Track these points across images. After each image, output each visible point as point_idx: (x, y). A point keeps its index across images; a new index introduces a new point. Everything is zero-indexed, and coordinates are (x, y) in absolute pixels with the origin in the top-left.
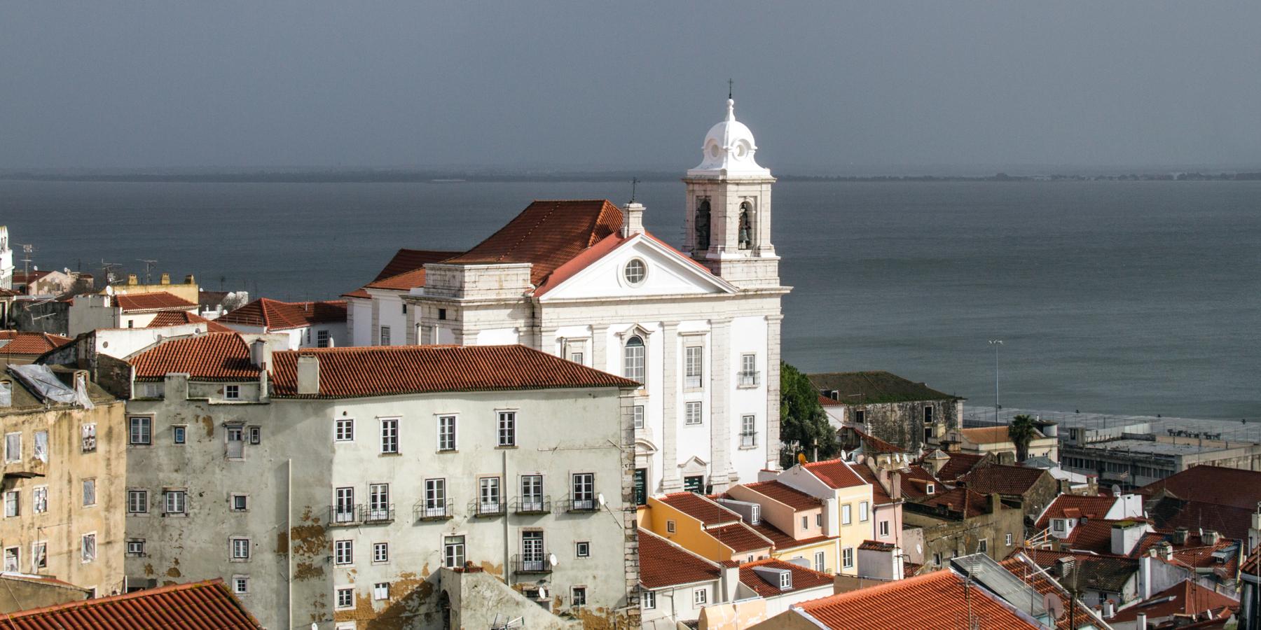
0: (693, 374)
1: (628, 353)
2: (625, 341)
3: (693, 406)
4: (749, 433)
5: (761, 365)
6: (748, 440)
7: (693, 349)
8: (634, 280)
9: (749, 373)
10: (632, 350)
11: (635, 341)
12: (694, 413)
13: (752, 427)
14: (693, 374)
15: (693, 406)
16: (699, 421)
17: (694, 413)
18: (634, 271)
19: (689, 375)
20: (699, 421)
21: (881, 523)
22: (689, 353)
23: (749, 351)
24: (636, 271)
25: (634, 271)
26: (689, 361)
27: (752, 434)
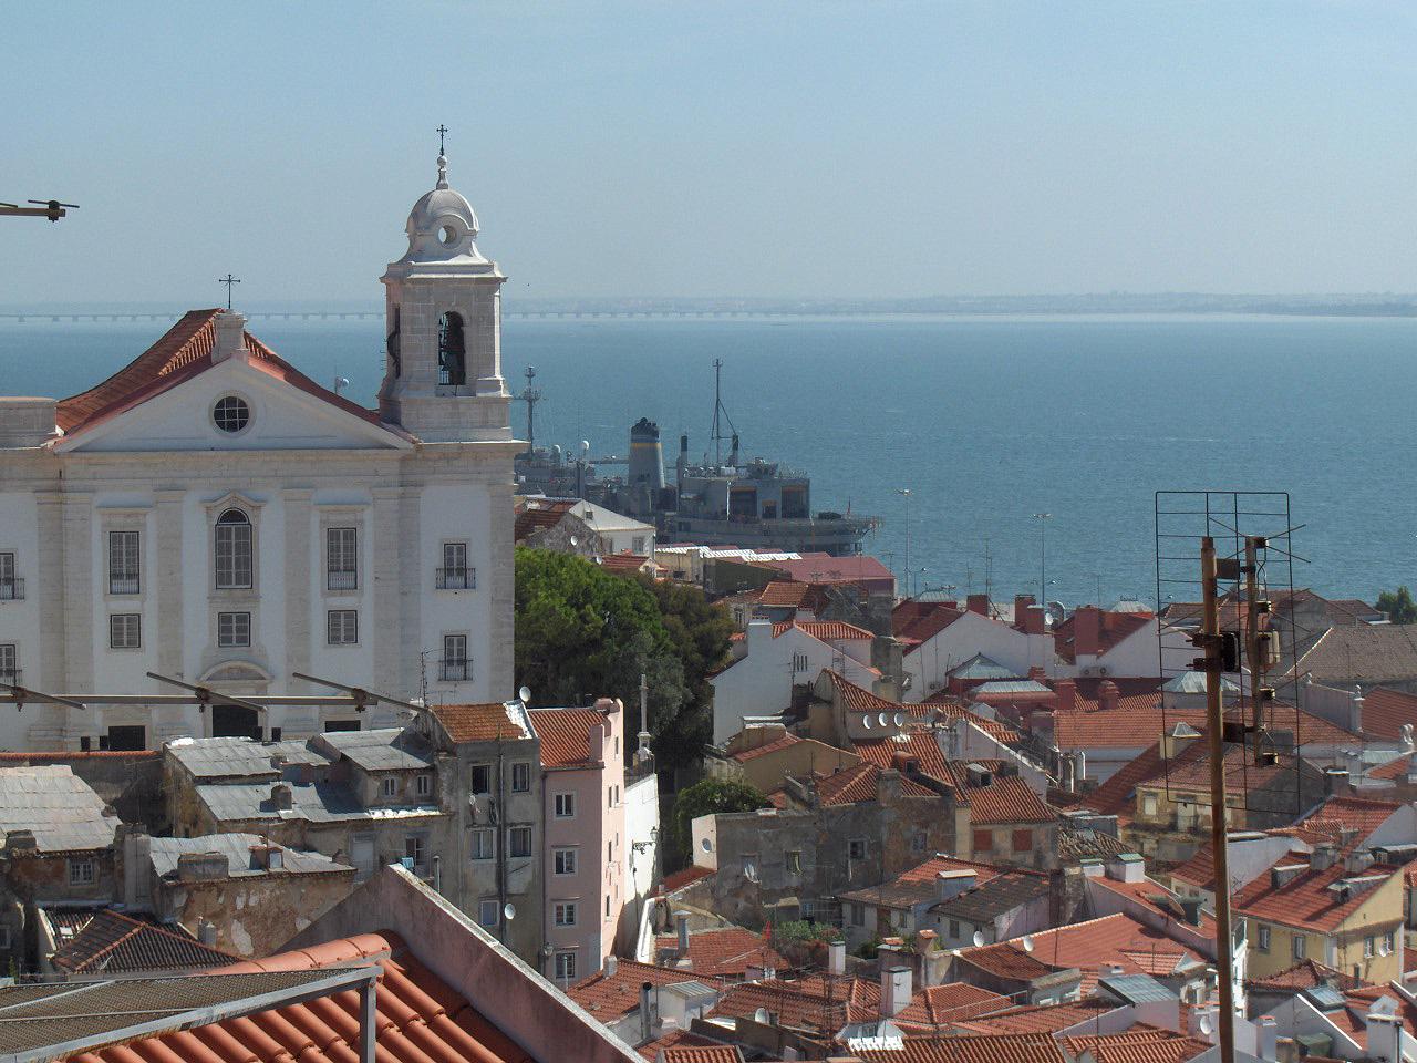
0: (342, 567)
1: (221, 534)
2: (216, 515)
3: (342, 616)
4: (456, 656)
5: (479, 558)
6: (456, 671)
7: (341, 532)
8: (233, 427)
9: (456, 568)
10: (229, 530)
11: (233, 516)
12: (342, 628)
13: (463, 651)
14: (342, 567)
15: (342, 616)
16: (352, 638)
17: (342, 628)
18: (232, 414)
19: (331, 570)
20: (352, 638)
21: (559, 799)
22: (332, 535)
23: (455, 536)
24: (231, 415)
25: (232, 414)
26: (332, 549)
27: (463, 662)
